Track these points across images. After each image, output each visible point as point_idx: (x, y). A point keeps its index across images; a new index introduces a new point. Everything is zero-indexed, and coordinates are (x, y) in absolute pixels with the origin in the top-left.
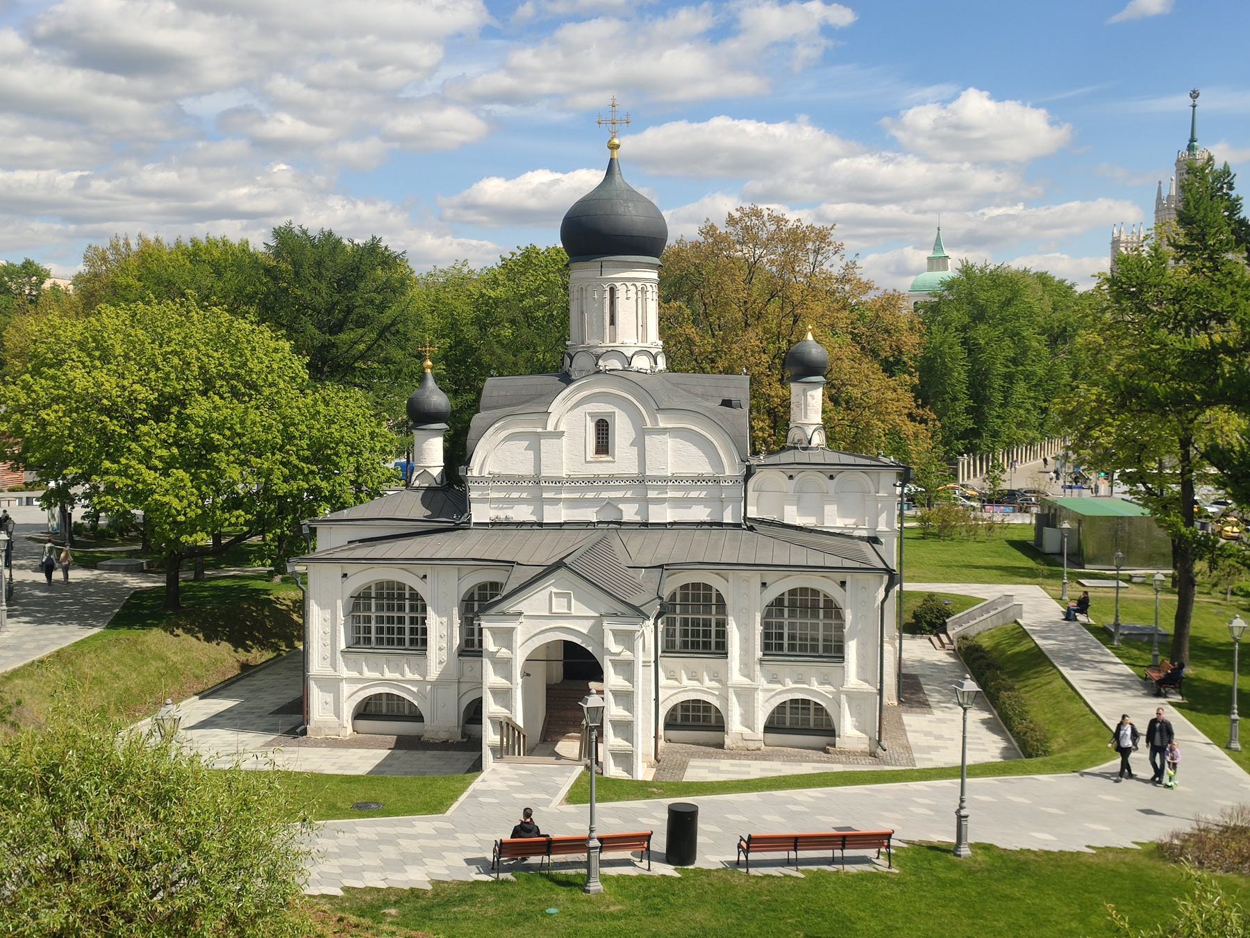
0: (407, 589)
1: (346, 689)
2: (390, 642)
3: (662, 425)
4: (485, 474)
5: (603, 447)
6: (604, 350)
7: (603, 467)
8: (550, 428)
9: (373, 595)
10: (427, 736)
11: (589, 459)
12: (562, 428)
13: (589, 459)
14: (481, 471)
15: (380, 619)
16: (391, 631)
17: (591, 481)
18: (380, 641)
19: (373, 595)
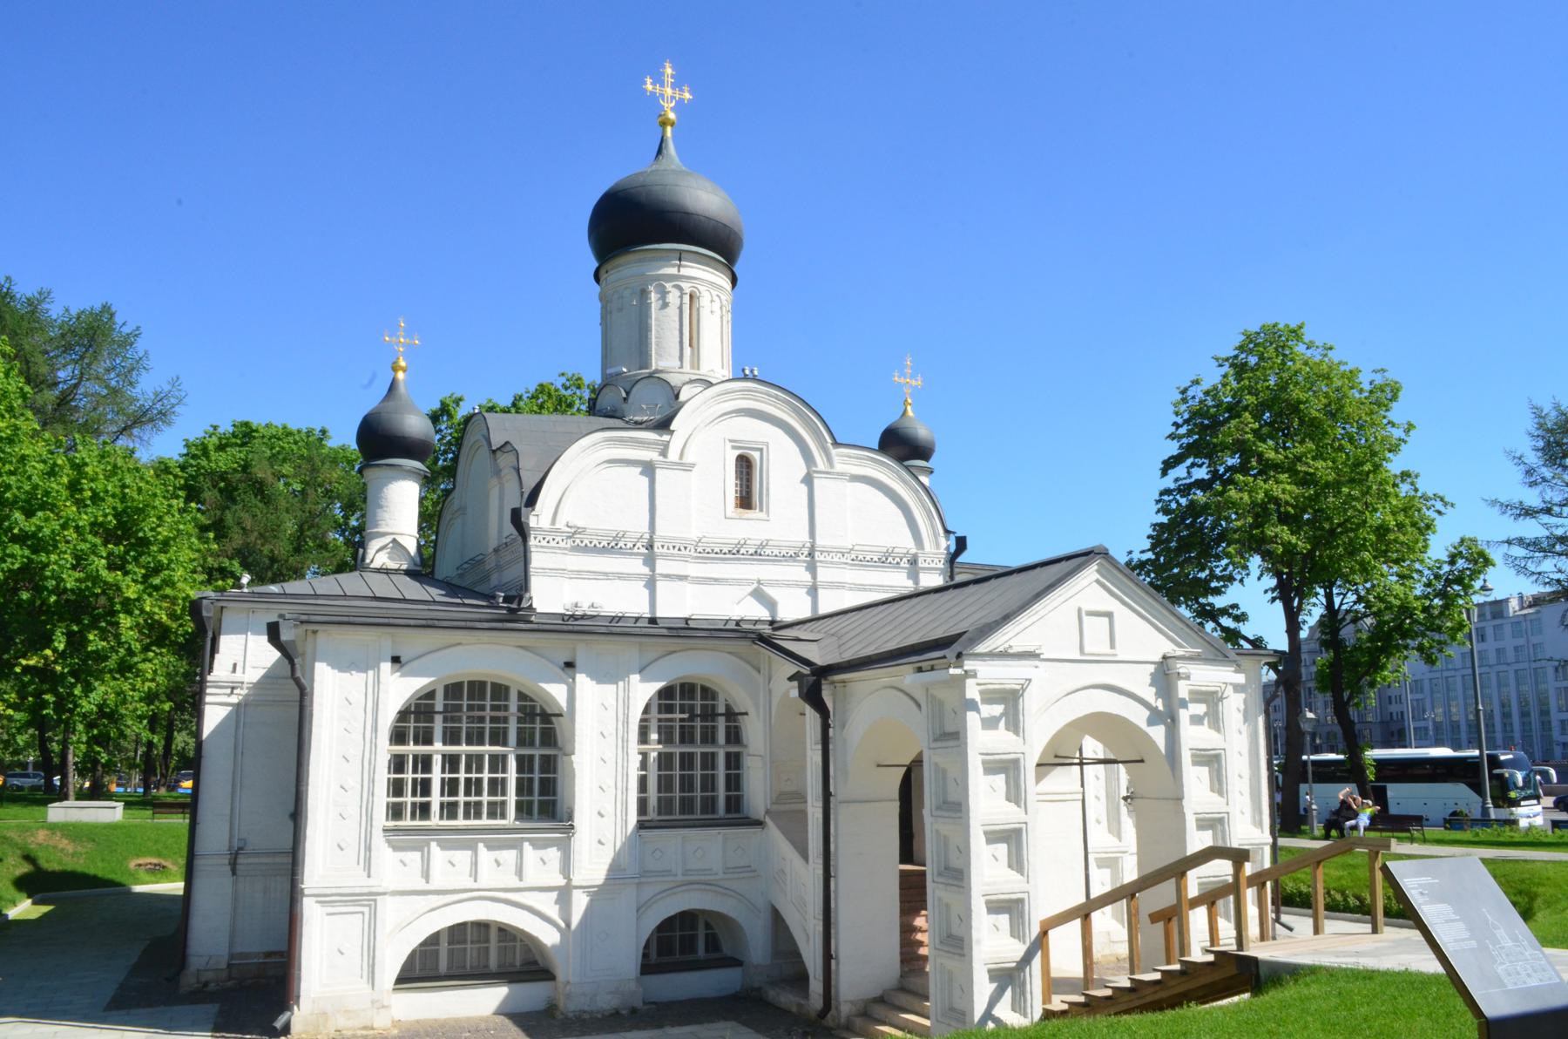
0: (513, 696)
1: (390, 911)
2: (473, 810)
3: (839, 467)
4: (560, 525)
5: (745, 501)
6: (687, 378)
7: (749, 528)
8: (673, 455)
9: (439, 707)
10: (570, 1005)
11: (729, 514)
12: (688, 459)
13: (729, 514)
14: (553, 521)
15: (451, 762)
16: (473, 786)
17: (735, 553)
18: (450, 810)
19: (439, 707)
